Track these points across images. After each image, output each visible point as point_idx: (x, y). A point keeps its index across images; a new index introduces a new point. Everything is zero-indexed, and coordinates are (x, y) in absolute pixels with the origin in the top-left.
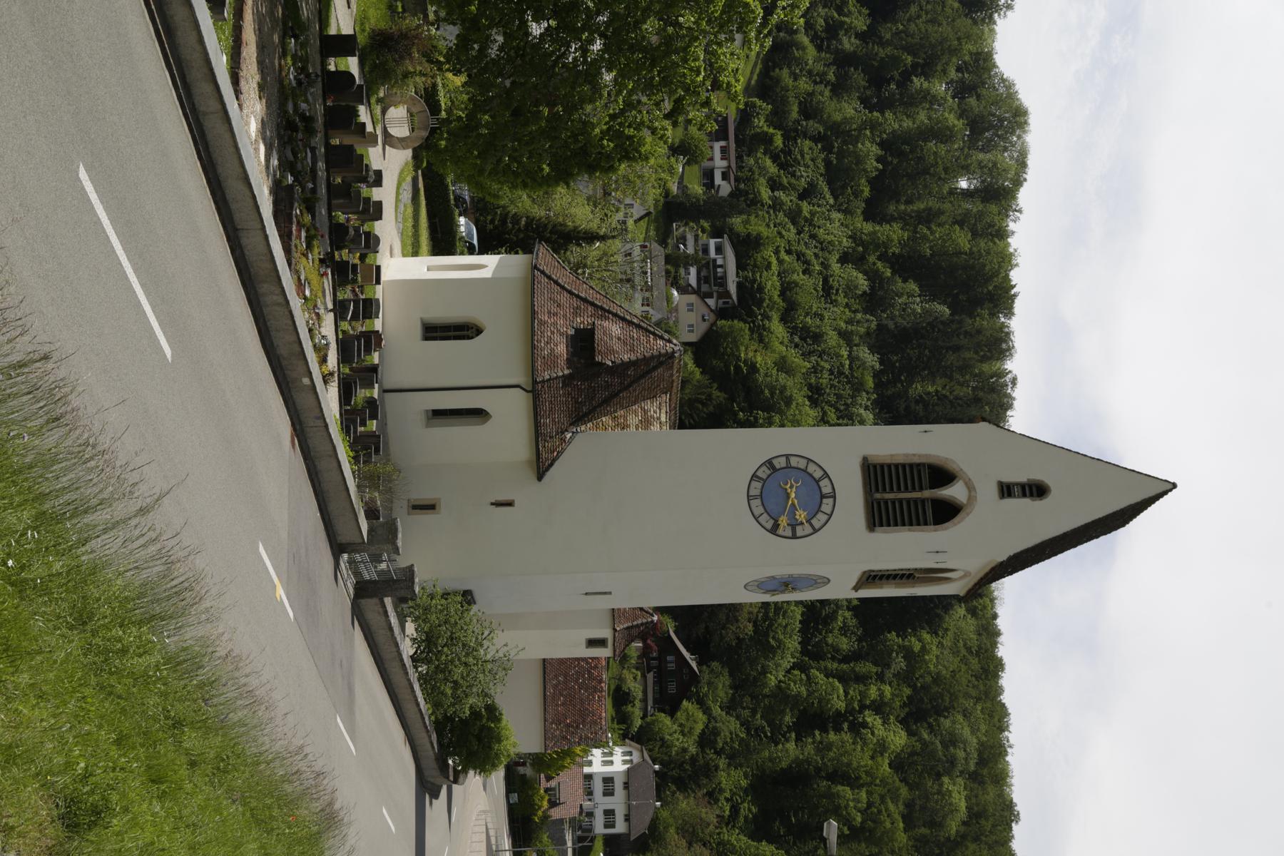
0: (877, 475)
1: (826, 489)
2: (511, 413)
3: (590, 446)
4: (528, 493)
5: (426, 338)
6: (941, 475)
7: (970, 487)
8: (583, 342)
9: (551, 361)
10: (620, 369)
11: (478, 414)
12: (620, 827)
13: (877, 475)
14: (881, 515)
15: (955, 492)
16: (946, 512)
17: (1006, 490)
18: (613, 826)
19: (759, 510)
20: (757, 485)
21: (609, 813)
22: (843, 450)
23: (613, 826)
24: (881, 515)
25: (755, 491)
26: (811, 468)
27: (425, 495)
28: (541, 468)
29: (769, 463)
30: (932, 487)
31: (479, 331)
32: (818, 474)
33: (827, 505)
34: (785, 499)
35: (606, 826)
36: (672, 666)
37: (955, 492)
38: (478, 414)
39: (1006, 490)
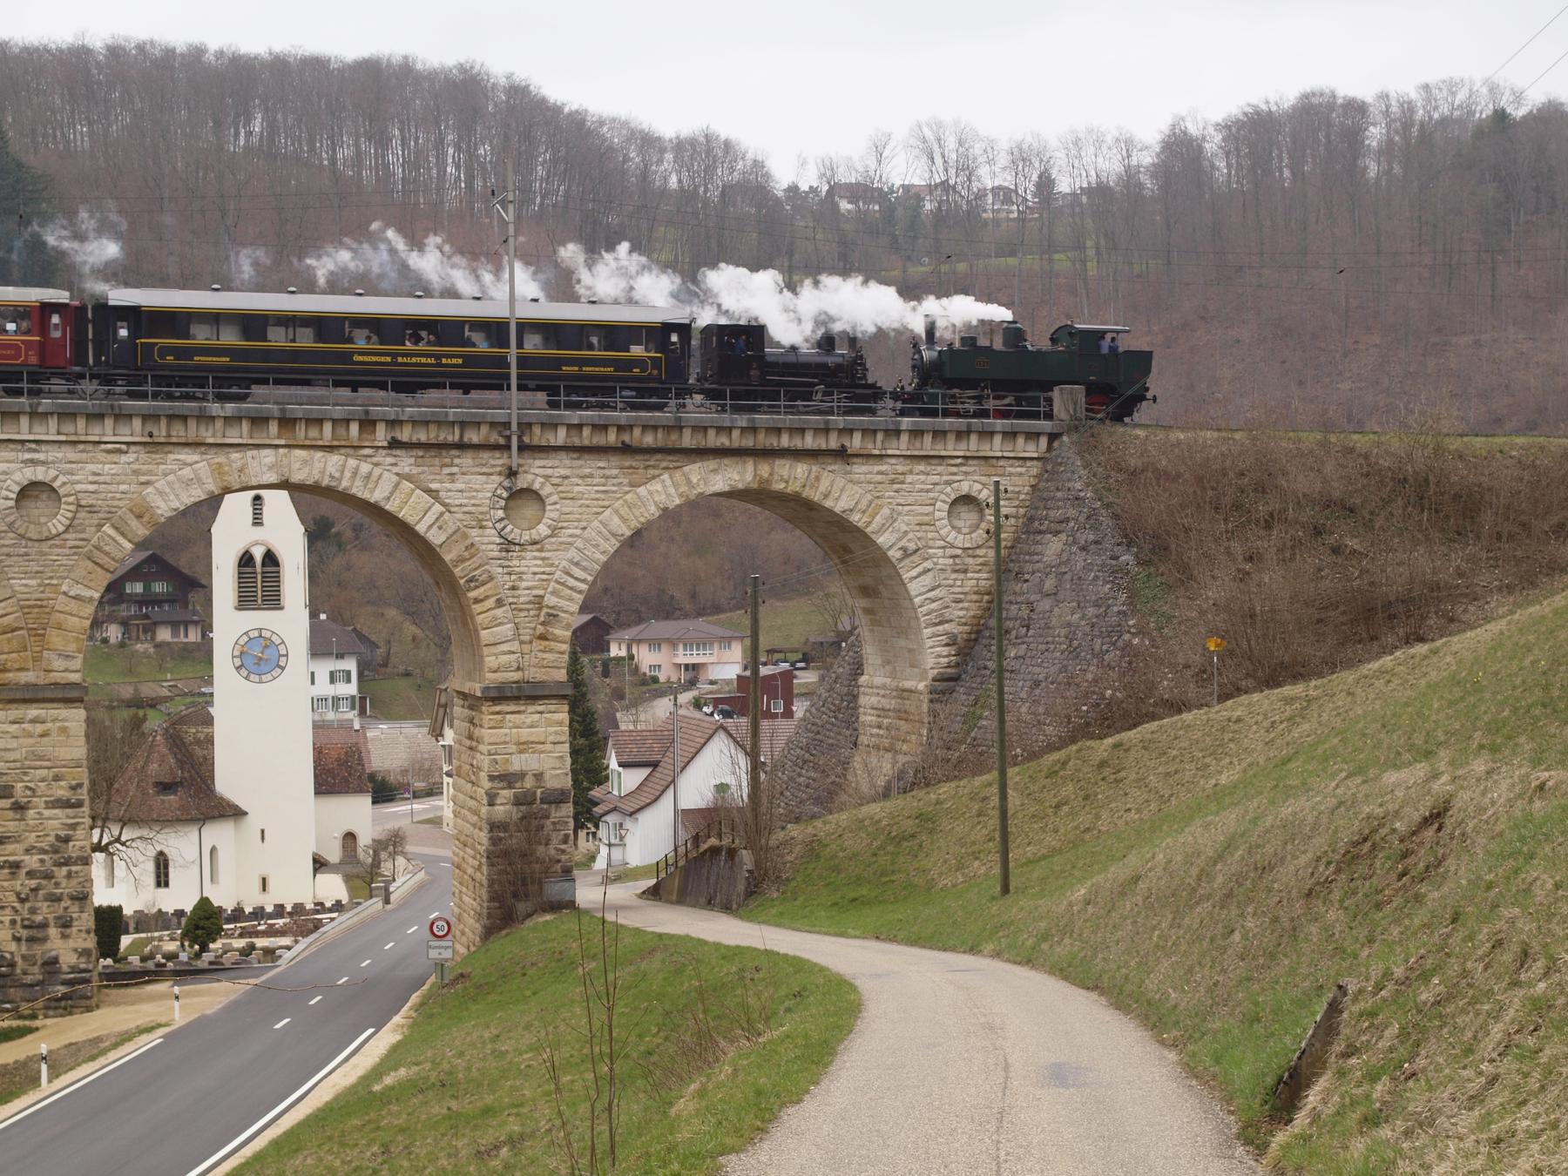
0: (245, 601)
1: (256, 634)
2: (218, 834)
3: (226, 783)
4: (253, 823)
5: (167, 885)
6: (246, 560)
7: (256, 543)
8: (165, 787)
9: (183, 808)
10: (181, 764)
11: (213, 850)
12: (351, 665)
13: (245, 601)
14: (272, 600)
15: (258, 553)
16: (271, 558)
17: (257, 521)
18: (349, 673)
19: (269, 677)
20: (252, 677)
21: (333, 678)
22: (230, 623)
23: (349, 673)
24: (272, 600)
25: (257, 678)
26: (242, 642)
27: (258, 884)
28: (237, 813)
29: (237, 668)
30: (254, 566)
31: (161, 853)
32: (245, 638)
33: (268, 634)
34: (260, 659)
35: (349, 681)
36: (138, 588)
37: (258, 553)
38: (213, 850)
39: (257, 521)
